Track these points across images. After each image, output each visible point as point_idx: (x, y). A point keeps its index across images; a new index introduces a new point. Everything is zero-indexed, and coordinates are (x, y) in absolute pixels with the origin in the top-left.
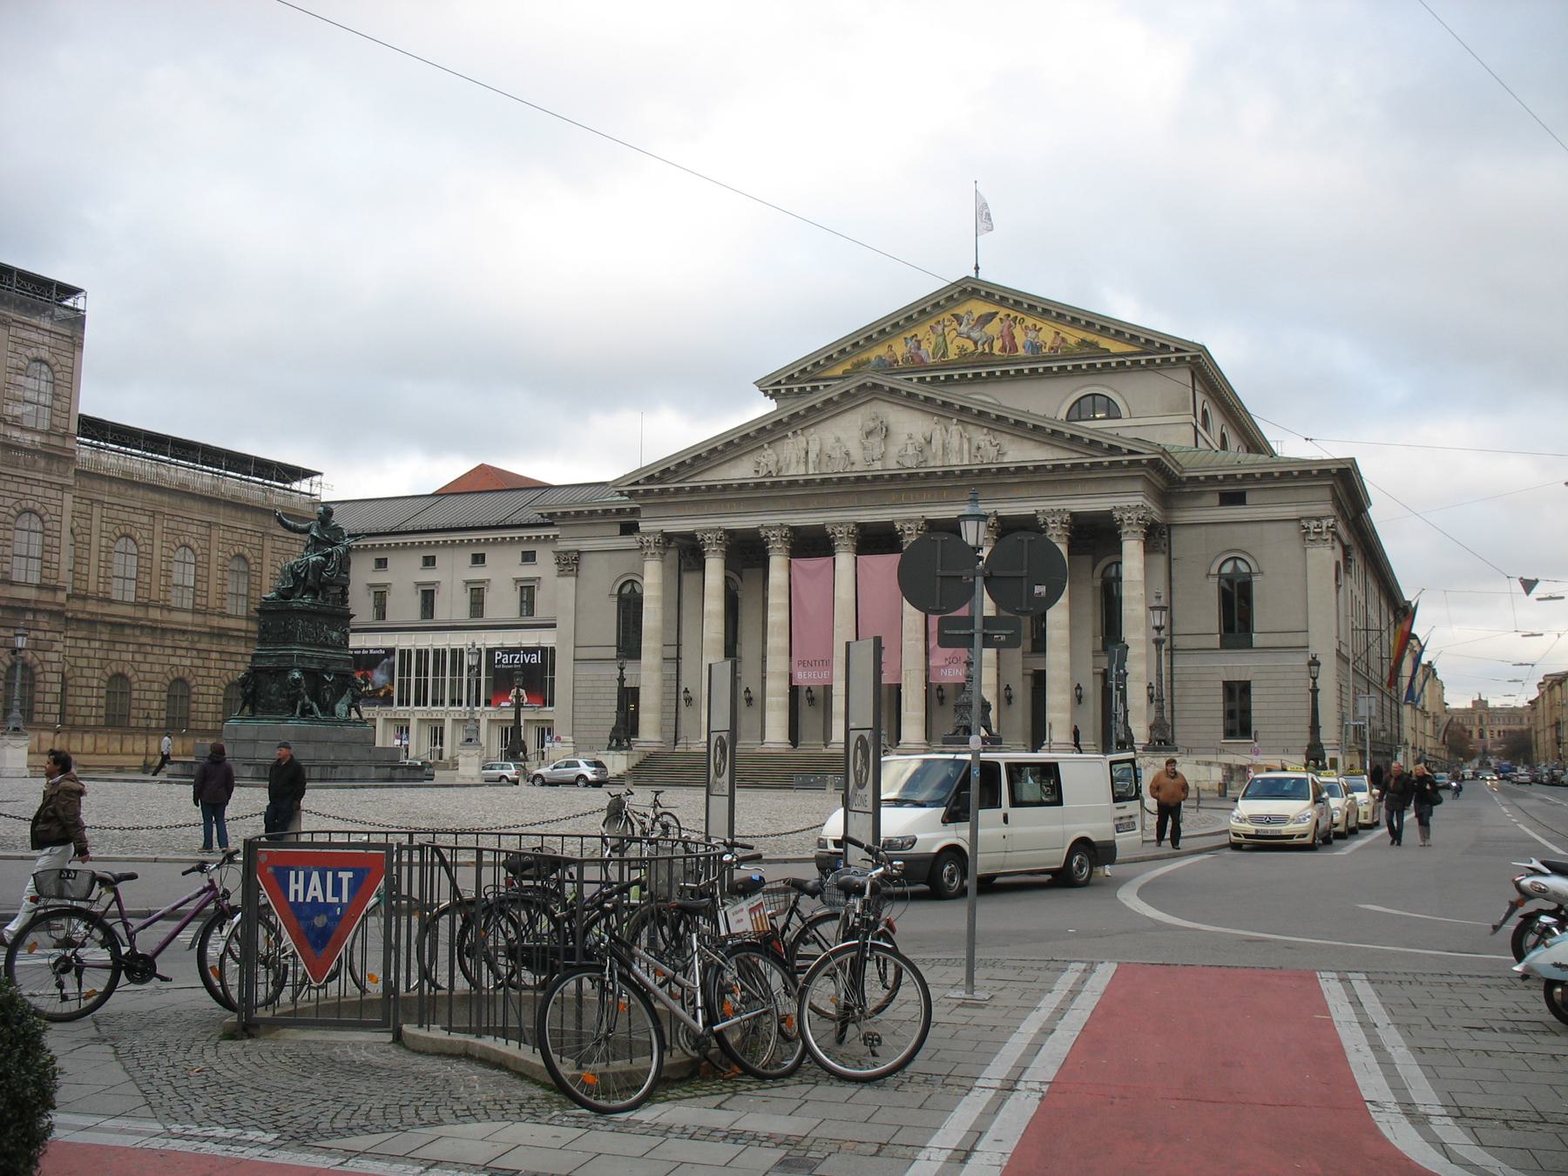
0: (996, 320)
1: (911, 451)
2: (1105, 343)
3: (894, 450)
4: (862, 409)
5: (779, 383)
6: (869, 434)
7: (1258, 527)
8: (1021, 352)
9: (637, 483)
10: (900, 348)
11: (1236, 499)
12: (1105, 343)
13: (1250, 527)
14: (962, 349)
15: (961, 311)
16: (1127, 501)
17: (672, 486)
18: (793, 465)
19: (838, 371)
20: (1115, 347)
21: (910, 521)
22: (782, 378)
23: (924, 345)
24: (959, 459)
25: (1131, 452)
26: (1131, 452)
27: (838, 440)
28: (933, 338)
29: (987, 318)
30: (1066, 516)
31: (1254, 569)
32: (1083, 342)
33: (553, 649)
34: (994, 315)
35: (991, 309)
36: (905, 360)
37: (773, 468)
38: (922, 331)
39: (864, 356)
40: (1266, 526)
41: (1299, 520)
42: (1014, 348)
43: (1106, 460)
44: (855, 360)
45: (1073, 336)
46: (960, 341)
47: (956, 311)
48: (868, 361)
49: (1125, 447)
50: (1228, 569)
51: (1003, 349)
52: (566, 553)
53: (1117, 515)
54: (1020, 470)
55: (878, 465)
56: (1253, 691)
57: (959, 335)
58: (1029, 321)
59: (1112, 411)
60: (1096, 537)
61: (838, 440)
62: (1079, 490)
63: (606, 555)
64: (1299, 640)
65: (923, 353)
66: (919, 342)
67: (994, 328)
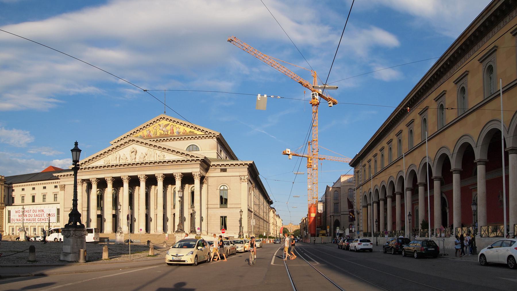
2: (196, 131)
3: (137, 157)
8: (175, 134)
11: (224, 170)
14: (161, 133)
15: (160, 123)
16: (196, 170)
17: (83, 167)
20: (199, 133)
23: (151, 132)
25: (197, 157)
26: (197, 157)
29: (167, 125)
32: (190, 132)
35: (167, 122)
36: (147, 136)
38: (151, 128)
42: (173, 133)
45: (188, 130)
47: (159, 123)
51: (171, 133)
53: (193, 174)
55: (134, 161)
58: (178, 125)
59: (197, 149)
60: (188, 179)
65: (151, 134)
67: (168, 128)
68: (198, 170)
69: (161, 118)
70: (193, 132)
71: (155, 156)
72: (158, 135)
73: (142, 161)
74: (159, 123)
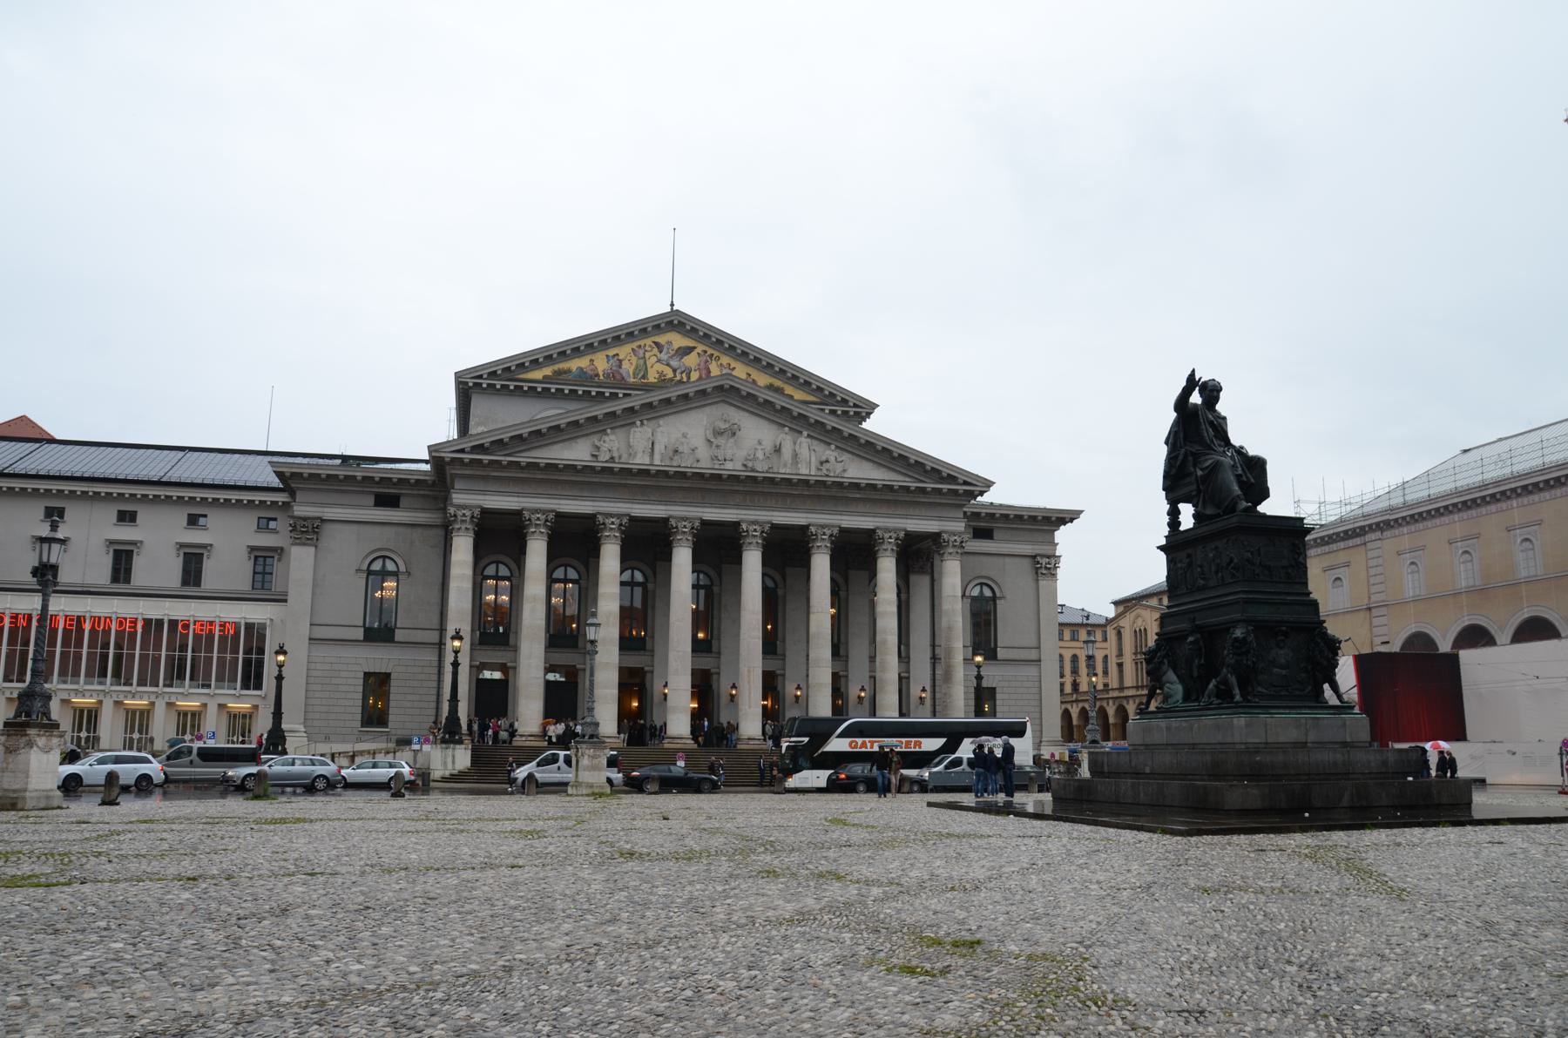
0: (694, 354)
1: (760, 455)
2: (789, 390)
4: (707, 410)
5: (480, 377)
6: (718, 433)
7: (1001, 560)
9: (462, 451)
10: (601, 363)
12: (789, 390)
13: (995, 559)
14: (661, 374)
15: (662, 339)
19: (537, 375)
20: (799, 395)
21: (754, 523)
22: (485, 373)
23: (625, 365)
25: (966, 483)
26: (966, 483)
27: (684, 436)
28: (634, 360)
30: (902, 535)
32: (771, 387)
33: (263, 627)
34: (692, 349)
36: (607, 376)
37: (616, 454)
38: (624, 351)
39: (564, 366)
40: (1007, 560)
41: (1034, 557)
44: (556, 367)
45: (763, 380)
46: (659, 367)
47: (657, 339)
48: (569, 371)
49: (962, 478)
50: (976, 592)
53: (945, 536)
54: (873, 487)
55: (729, 465)
57: (659, 361)
58: (725, 360)
61: (684, 436)
62: (911, 511)
64: (1033, 655)
67: (691, 360)
68: (960, 526)
70: (779, 391)
72: (652, 378)
73: (761, 468)
74: (657, 339)
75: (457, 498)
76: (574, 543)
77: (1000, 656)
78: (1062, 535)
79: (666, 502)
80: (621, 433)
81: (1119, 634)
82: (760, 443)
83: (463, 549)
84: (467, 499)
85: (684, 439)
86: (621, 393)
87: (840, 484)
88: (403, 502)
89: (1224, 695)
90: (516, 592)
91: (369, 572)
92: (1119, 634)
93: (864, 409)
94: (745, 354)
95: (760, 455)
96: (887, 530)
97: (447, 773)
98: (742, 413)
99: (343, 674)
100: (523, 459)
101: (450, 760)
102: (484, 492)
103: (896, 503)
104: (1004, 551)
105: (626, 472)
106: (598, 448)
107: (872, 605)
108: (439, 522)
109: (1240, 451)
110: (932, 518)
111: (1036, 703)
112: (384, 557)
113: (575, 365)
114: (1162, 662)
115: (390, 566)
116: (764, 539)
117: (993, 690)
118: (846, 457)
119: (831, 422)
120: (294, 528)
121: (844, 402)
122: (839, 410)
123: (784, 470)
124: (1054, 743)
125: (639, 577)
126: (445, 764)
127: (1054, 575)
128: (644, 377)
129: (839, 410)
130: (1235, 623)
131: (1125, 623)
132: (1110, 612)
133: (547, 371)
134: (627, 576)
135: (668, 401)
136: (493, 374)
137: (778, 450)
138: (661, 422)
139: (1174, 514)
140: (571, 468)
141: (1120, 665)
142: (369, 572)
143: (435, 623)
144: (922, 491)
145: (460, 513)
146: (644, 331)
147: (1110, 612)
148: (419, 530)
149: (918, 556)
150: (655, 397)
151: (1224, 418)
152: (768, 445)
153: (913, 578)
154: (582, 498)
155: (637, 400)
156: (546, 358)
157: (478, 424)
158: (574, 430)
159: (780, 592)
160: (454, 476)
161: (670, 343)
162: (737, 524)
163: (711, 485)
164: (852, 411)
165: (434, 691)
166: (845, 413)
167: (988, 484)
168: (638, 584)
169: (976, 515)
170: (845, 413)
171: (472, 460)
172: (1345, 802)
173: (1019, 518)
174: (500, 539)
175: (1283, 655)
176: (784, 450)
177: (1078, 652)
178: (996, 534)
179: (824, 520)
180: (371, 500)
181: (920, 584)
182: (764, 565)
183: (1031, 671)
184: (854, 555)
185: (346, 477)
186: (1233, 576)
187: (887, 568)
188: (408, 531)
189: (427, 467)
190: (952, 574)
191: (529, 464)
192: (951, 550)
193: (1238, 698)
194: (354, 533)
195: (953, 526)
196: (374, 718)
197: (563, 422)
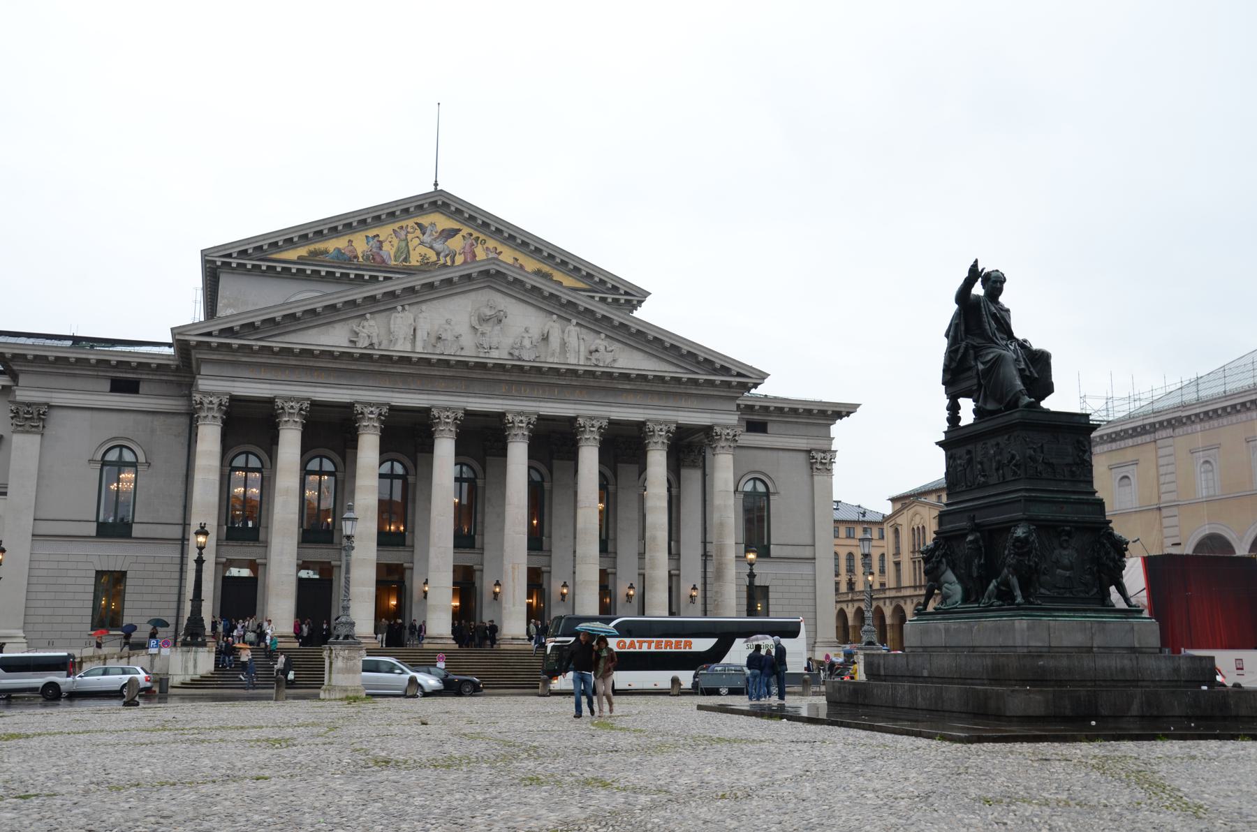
0: (459, 237)
1: (527, 343)
2: (558, 276)
4: (473, 295)
5: (230, 255)
6: (484, 320)
7: (775, 454)
9: (209, 334)
10: (360, 244)
12: (558, 276)
13: (769, 452)
14: (424, 257)
15: (425, 220)
18: (400, 342)
19: (292, 255)
20: (568, 282)
21: (520, 413)
22: (234, 251)
23: (386, 246)
24: (576, 358)
25: (739, 375)
26: (739, 375)
27: (448, 322)
28: (395, 241)
30: (673, 428)
31: (772, 490)
32: (538, 273)
36: (367, 258)
37: (375, 341)
38: (385, 232)
39: (320, 246)
40: (781, 453)
41: (809, 451)
43: (718, 378)
44: (312, 247)
45: (531, 265)
47: (419, 220)
48: (326, 252)
49: (735, 369)
50: (749, 487)
52: (29, 405)
53: (718, 429)
54: (643, 378)
55: (495, 354)
56: (771, 595)
57: (422, 243)
58: (491, 243)
61: (448, 322)
62: (683, 404)
63: (88, 414)
66: (381, 242)
67: (456, 243)
68: (733, 419)
69: (435, 203)
70: (547, 276)
71: (582, 349)
72: (414, 261)
73: (528, 357)
74: (419, 220)
75: (204, 384)
76: (331, 433)
77: (773, 553)
78: (839, 429)
79: (429, 392)
80: (381, 318)
81: (896, 532)
82: (527, 331)
83: (209, 438)
84: (215, 385)
85: (447, 326)
86: (381, 276)
87: (610, 375)
88: (143, 387)
89: (1005, 595)
90: (267, 485)
91: (104, 463)
92: (896, 532)
93: (633, 297)
94: (512, 237)
95: (527, 343)
96: (658, 422)
97: (188, 679)
98: (508, 299)
99: (71, 573)
100: (276, 343)
101: (191, 664)
102: (233, 378)
103: (668, 394)
104: (779, 445)
105: (387, 359)
106: (357, 334)
107: (642, 500)
108: (183, 409)
109: (1023, 345)
110: (704, 410)
111: (811, 602)
112: (121, 447)
113: (332, 245)
114: (940, 561)
115: (128, 456)
116: (531, 431)
117: (765, 589)
118: (616, 346)
119: (601, 310)
120: (16, 415)
121: (615, 288)
122: (610, 297)
123: (552, 358)
124: (829, 644)
125: (399, 469)
126: (186, 668)
127: (830, 470)
128: (406, 260)
129: (610, 297)
130: (1016, 523)
131: (903, 520)
132: (887, 509)
133: (303, 251)
134: (386, 468)
135: (430, 286)
136: (243, 253)
137: (545, 338)
138: (424, 307)
139: (954, 409)
140: (328, 354)
141: (897, 564)
142: (104, 463)
143: (178, 517)
144: (695, 382)
145: (206, 400)
146: (406, 211)
147: (887, 509)
148: (162, 418)
149: (689, 448)
150: (417, 281)
151: (947, 335)
152: (535, 333)
153: (685, 473)
154: (338, 386)
155: (398, 284)
156: (301, 237)
157: (227, 306)
158: (329, 314)
159: (546, 485)
160: (200, 362)
161: (433, 225)
162: (502, 415)
163: (477, 374)
164: (623, 299)
165: (176, 590)
166: (616, 301)
167: (763, 376)
168: (398, 477)
169: (750, 408)
170: (616, 301)
171: (220, 345)
172: (1135, 710)
173: (794, 411)
174: (250, 427)
175: (1067, 555)
176: (551, 338)
177: (853, 550)
178: (770, 428)
179: (593, 412)
180: (107, 385)
181: (692, 478)
182: (530, 457)
183: (806, 569)
184: (623, 447)
185: (78, 360)
186: (1015, 473)
187: (657, 461)
188: (149, 418)
189: (170, 351)
190: (724, 468)
191: (282, 349)
192: (723, 444)
193: (1019, 600)
194: (87, 420)
195: (725, 418)
196: (107, 620)
197: (319, 306)
